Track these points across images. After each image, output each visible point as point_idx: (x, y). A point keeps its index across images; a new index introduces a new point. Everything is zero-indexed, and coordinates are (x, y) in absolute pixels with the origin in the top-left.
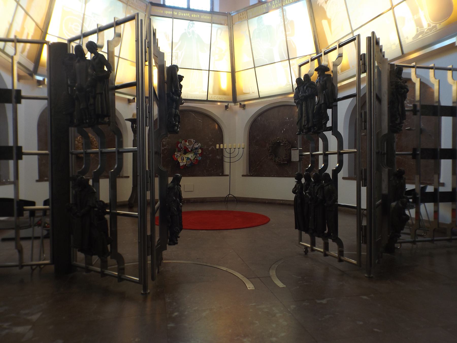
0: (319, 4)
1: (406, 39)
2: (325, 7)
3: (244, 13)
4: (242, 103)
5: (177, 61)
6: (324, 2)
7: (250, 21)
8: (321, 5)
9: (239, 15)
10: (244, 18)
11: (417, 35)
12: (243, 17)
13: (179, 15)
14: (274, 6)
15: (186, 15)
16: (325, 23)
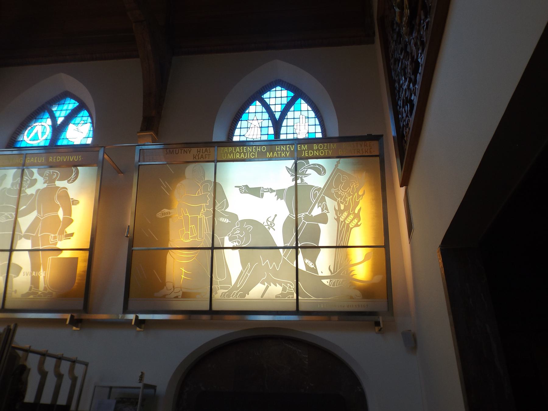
1: (13, 293)
11: (28, 294)
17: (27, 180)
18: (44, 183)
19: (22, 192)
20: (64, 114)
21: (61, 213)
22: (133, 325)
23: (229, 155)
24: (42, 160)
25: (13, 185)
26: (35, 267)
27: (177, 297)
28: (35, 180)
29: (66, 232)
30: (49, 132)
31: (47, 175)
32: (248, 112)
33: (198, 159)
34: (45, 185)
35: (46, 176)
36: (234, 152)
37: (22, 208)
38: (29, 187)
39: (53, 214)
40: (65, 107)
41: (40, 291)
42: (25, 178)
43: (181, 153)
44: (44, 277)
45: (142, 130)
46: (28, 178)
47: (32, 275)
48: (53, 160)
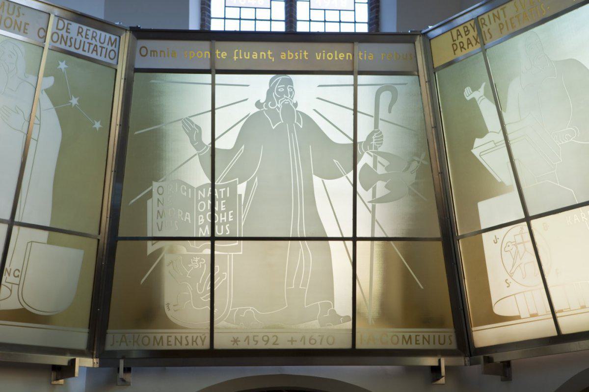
3: (470, 28)
4: (498, 358)
5: (234, 215)
9: (455, 38)
10: (474, 42)
12: (468, 39)
13: (235, 58)
15: (259, 56)
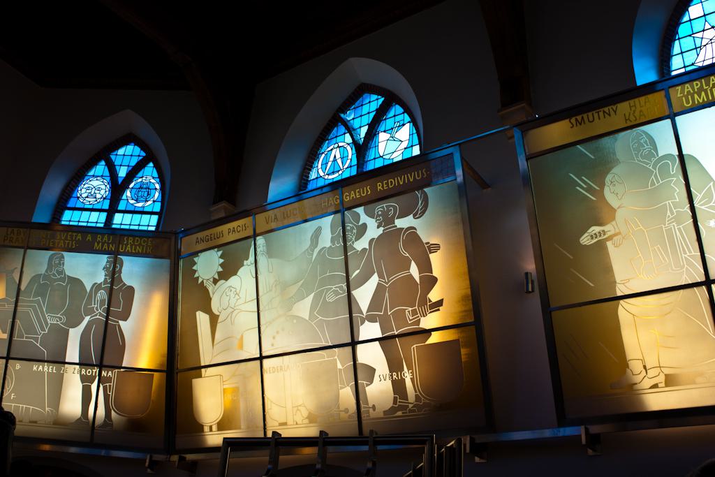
0: (198, 278)
1: (371, 410)
2: (210, 289)
6: (212, 280)
7: (31, 253)
8: (203, 281)
9: (9, 233)
11: (392, 410)
14: (98, 244)
16: (202, 319)
17: (352, 228)
18: (378, 227)
19: (348, 249)
20: (367, 119)
21: (414, 270)
22: (584, 445)
23: (696, 96)
24: (367, 192)
25: (333, 240)
26: (394, 365)
27: (655, 386)
28: (365, 226)
29: (430, 301)
30: (351, 152)
31: (380, 213)
32: (688, 19)
33: (636, 120)
34: (381, 230)
35: (378, 216)
36: (705, 88)
37: (354, 274)
38: (357, 239)
39: (402, 274)
40: (365, 109)
41: (411, 403)
42: (349, 226)
43: (599, 119)
44: (412, 380)
45: (505, 105)
46: (352, 223)
47: (392, 378)
48: (383, 187)
